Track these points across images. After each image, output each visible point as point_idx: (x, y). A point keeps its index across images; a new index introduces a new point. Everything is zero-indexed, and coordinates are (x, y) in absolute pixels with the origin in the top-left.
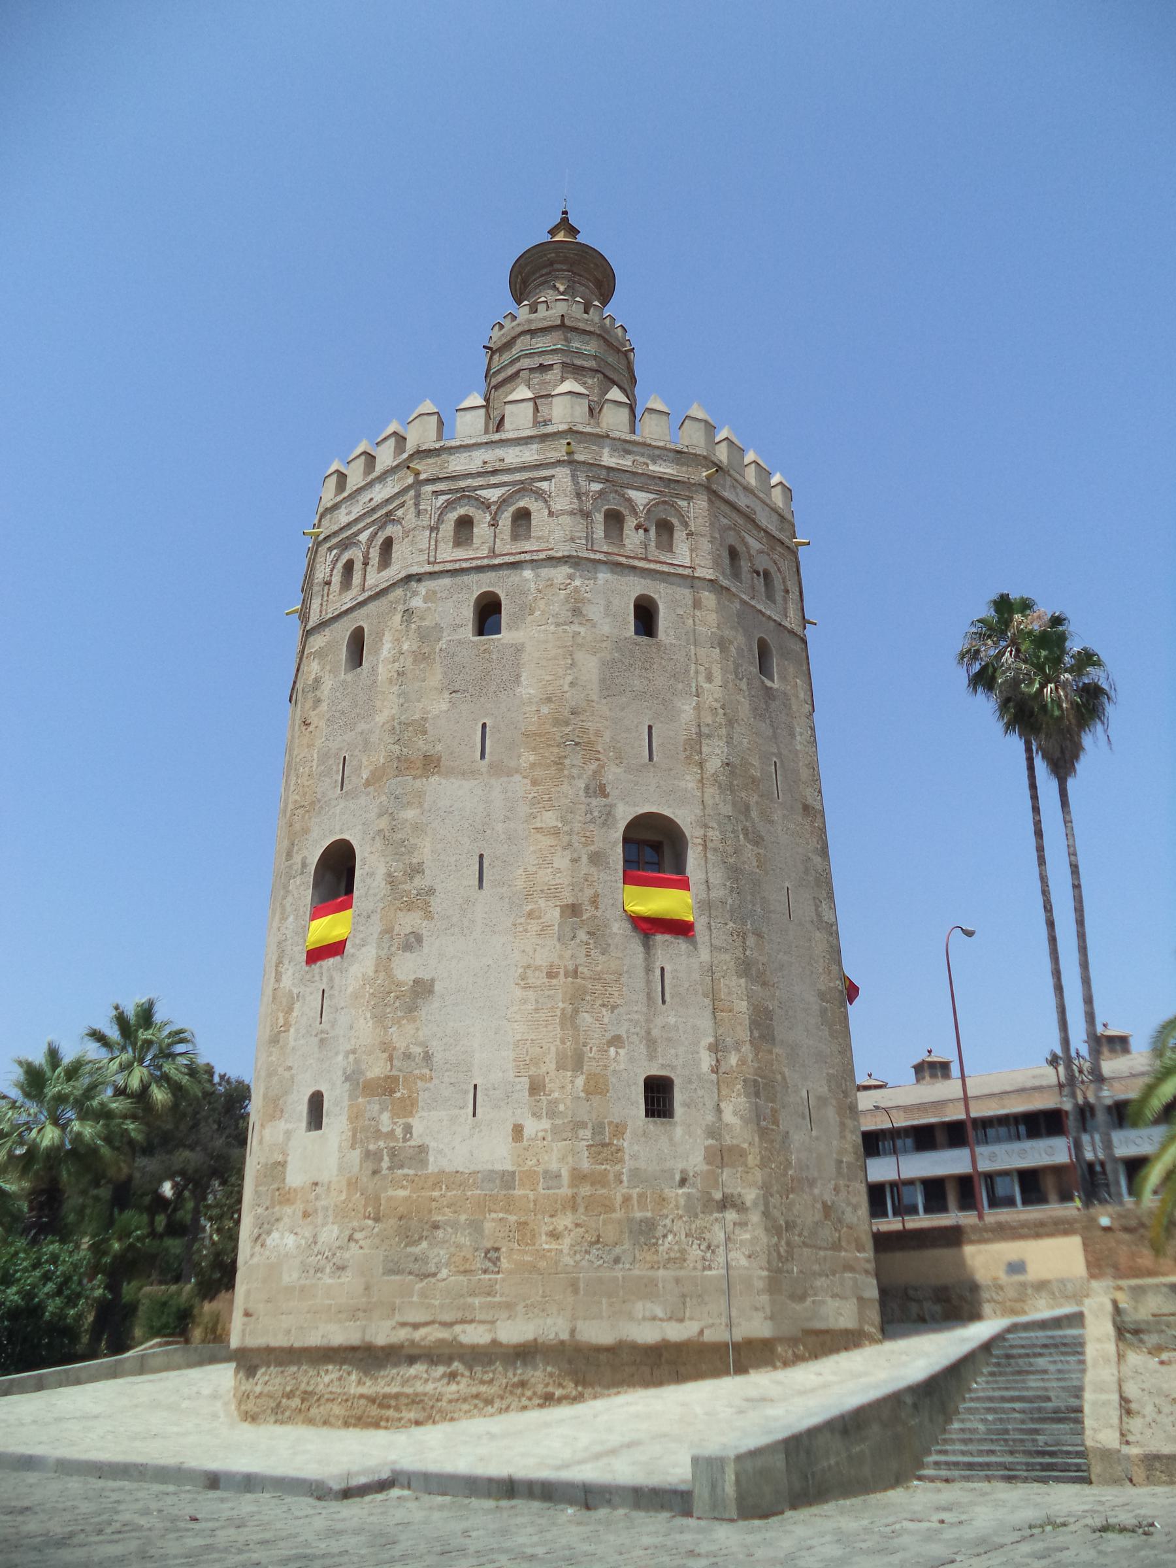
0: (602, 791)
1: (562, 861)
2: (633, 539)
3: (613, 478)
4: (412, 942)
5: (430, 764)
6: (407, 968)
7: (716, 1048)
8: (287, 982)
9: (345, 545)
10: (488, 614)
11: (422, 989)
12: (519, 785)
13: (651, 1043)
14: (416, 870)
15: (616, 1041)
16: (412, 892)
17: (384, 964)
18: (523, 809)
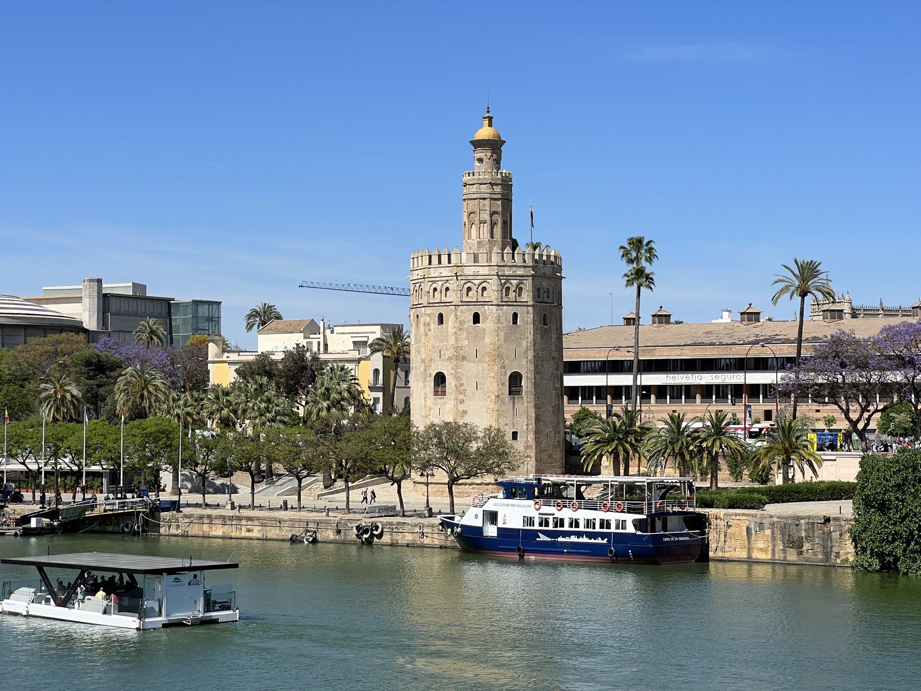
0: (504, 367)
1: (495, 385)
2: (512, 295)
3: (508, 278)
4: (462, 401)
5: (464, 358)
6: (461, 408)
7: (527, 425)
8: (428, 403)
9: (434, 282)
10: (476, 318)
11: (465, 412)
12: (485, 365)
13: (513, 424)
14: (462, 385)
15: (506, 425)
16: (460, 389)
17: (456, 406)
18: (486, 372)
